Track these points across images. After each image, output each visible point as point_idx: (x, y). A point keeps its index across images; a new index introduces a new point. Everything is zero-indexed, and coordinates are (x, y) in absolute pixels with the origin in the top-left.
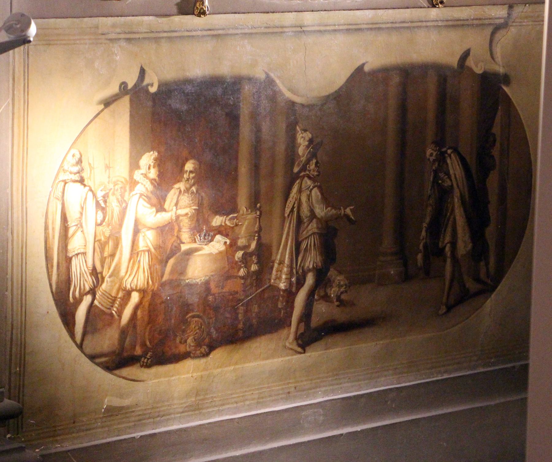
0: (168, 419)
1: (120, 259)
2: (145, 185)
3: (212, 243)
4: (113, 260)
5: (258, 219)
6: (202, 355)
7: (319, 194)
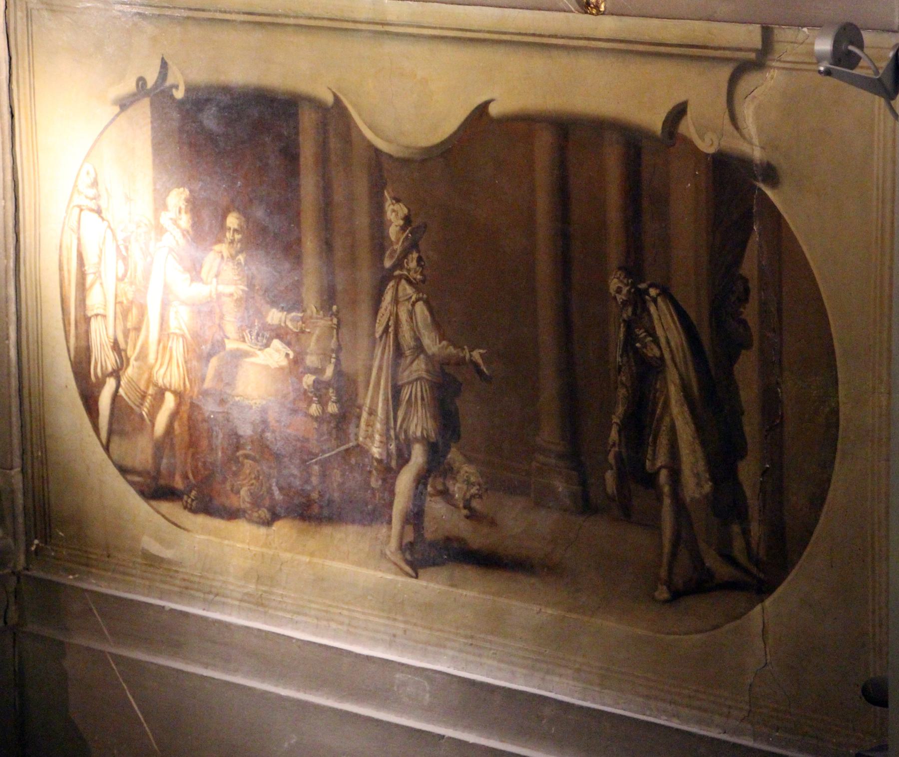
0: (224, 603)
1: (147, 337)
2: (174, 237)
3: (267, 350)
4: (138, 336)
5: (335, 331)
6: (261, 521)
7: (427, 313)
